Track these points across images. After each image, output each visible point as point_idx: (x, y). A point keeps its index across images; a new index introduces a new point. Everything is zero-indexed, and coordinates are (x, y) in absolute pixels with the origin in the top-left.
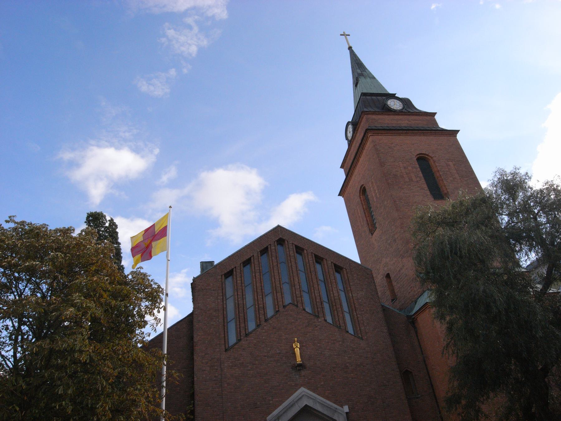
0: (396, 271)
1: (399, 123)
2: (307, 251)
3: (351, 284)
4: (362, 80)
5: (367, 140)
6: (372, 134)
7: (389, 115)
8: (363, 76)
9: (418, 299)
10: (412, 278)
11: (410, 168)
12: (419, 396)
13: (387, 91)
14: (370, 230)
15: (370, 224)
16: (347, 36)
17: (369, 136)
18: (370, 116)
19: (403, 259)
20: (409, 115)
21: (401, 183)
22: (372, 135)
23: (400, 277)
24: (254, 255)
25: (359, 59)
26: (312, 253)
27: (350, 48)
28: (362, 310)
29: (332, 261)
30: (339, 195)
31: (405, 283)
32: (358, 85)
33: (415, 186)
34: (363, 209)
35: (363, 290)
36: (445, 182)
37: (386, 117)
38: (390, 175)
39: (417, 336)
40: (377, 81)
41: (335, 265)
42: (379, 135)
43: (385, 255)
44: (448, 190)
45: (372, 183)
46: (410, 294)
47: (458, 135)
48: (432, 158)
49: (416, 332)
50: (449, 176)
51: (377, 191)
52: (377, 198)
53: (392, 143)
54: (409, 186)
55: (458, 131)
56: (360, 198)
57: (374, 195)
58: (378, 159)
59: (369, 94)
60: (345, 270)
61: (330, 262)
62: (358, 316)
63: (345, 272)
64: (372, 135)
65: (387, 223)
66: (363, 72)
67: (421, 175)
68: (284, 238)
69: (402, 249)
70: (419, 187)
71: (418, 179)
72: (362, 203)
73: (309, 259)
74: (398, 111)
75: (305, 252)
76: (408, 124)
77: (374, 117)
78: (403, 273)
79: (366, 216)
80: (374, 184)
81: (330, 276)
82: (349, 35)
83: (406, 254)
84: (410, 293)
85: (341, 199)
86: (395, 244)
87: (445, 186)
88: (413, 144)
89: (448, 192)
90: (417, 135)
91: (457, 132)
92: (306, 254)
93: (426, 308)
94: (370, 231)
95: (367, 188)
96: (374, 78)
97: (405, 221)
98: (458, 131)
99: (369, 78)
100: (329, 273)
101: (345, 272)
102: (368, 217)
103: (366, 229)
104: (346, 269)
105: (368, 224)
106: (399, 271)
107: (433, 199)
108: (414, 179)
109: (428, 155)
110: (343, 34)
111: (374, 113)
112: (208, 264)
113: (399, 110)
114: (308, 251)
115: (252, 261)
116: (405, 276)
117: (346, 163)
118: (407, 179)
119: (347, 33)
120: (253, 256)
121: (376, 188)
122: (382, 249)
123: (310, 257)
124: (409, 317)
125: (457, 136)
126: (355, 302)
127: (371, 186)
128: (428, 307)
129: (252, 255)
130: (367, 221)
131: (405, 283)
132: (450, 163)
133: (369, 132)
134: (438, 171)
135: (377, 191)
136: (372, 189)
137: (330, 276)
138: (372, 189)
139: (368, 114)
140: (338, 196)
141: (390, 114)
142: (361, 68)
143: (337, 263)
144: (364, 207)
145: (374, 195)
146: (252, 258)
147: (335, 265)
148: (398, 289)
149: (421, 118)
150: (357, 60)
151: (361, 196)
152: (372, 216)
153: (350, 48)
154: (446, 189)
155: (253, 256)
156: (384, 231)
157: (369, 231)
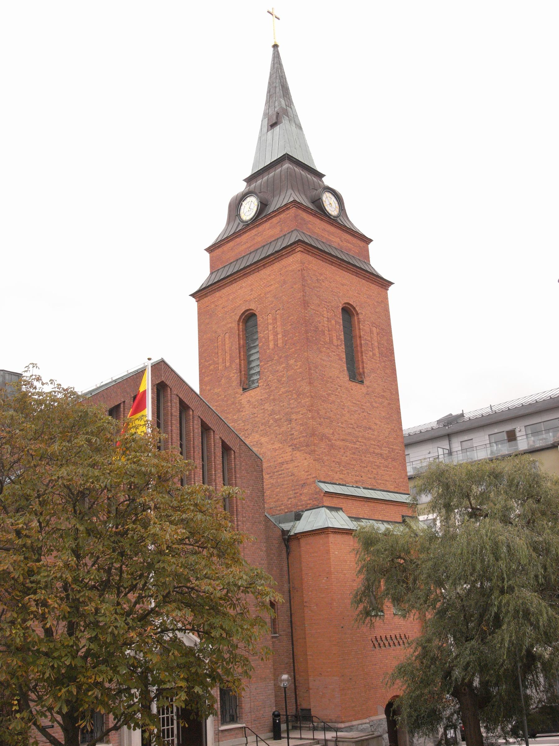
0: (275, 461)
1: (330, 238)
2: (193, 411)
3: (238, 475)
4: (285, 123)
5: (289, 254)
6: (302, 250)
7: (322, 220)
8: (288, 117)
9: (303, 511)
10: (302, 482)
11: (333, 322)
12: (277, 635)
13: (313, 162)
14: (241, 380)
15: (243, 372)
16: (276, 19)
17: (297, 250)
18: (300, 212)
19: (295, 452)
20: (343, 230)
21: (321, 342)
22: (302, 252)
23: (280, 473)
24: (126, 401)
25: (285, 79)
26: (199, 417)
27: (275, 46)
28: (244, 515)
29: (221, 435)
30: (193, 295)
31: (286, 483)
32: (277, 129)
33: (334, 352)
34: (239, 344)
35: (249, 488)
36: (364, 357)
37: (318, 221)
38: (311, 324)
39: (288, 559)
40: (303, 135)
41: (223, 442)
42: (310, 254)
43: (261, 431)
44: (365, 370)
45: (275, 319)
46: (290, 500)
47: (390, 288)
48: (357, 314)
49: (288, 554)
50: (370, 349)
51: (280, 336)
52: (276, 345)
53: (321, 274)
54: (328, 351)
55: (392, 283)
56: (239, 324)
57: (271, 337)
58: (302, 294)
59: (295, 160)
60: (233, 452)
61: (217, 437)
62: (239, 523)
63: (233, 456)
64: (302, 252)
65: (283, 390)
66: (287, 107)
67: (342, 337)
68: (168, 383)
69: (300, 438)
70: (338, 355)
71: (339, 343)
72: (239, 335)
73: (195, 426)
74: (332, 218)
75: (191, 411)
76: (339, 244)
77: (305, 215)
78: (288, 469)
79: (240, 357)
80: (278, 324)
81: (215, 458)
82: (279, 19)
83: (305, 447)
84: (290, 498)
85: (193, 304)
86: (288, 425)
87: (363, 362)
88: (343, 285)
89: (364, 372)
90: (350, 272)
91: (391, 283)
92: (191, 417)
93: (324, 532)
94: (241, 383)
95: (260, 320)
96: (301, 128)
97: (315, 401)
98: (392, 283)
99: (294, 125)
100: (214, 453)
101: (233, 456)
102: (244, 360)
103: (235, 376)
104: (234, 452)
105: (240, 372)
106: (282, 463)
107: (348, 378)
108: (335, 342)
109: (354, 308)
110: (271, 11)
111: (305, 209)
112: (13, 377)
113: (334, 217)
114: (194, 412)
115: (122, 410)
116: (290, 474)
117: (220, 250)
118: (327, 339)
119: (275, 13)
120: (124, 402)
121: (279, 330)
122: (257, 419)
123: (195, 422)
124: (284, 533)
125: (388, 290)
126: (238, 503)
127: (270, 321)
128: (326, 533)
129: (123, 400)
130: (240, 365)
131: (286, 483)
132: (374, 328)
133: (301, 245)
134: (360, 337)
135: (280, 336)
136: (270, 327)
137: (215, 458)
138: (270, 327)
139: (299, 208)
140: (191, 295)
141: (323, 219)
142: (285, 98)
143: (226, 441)
144: (242, 342)
145: (271, 337)
146: (122, 405)
147: (223, 442)
148: (270, 486)
149: (355, 240)
150: (282, 77)
151: (241, 324)
152: (249, 362)
153: (275, 46)
154: (363, 368)
155: (124, 402)
156: (272, 398)
157: (239, 381)
